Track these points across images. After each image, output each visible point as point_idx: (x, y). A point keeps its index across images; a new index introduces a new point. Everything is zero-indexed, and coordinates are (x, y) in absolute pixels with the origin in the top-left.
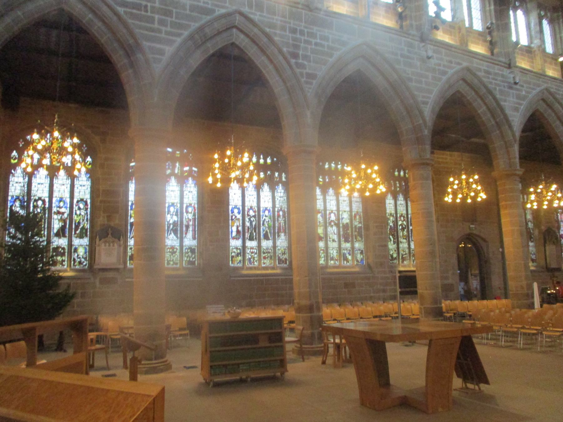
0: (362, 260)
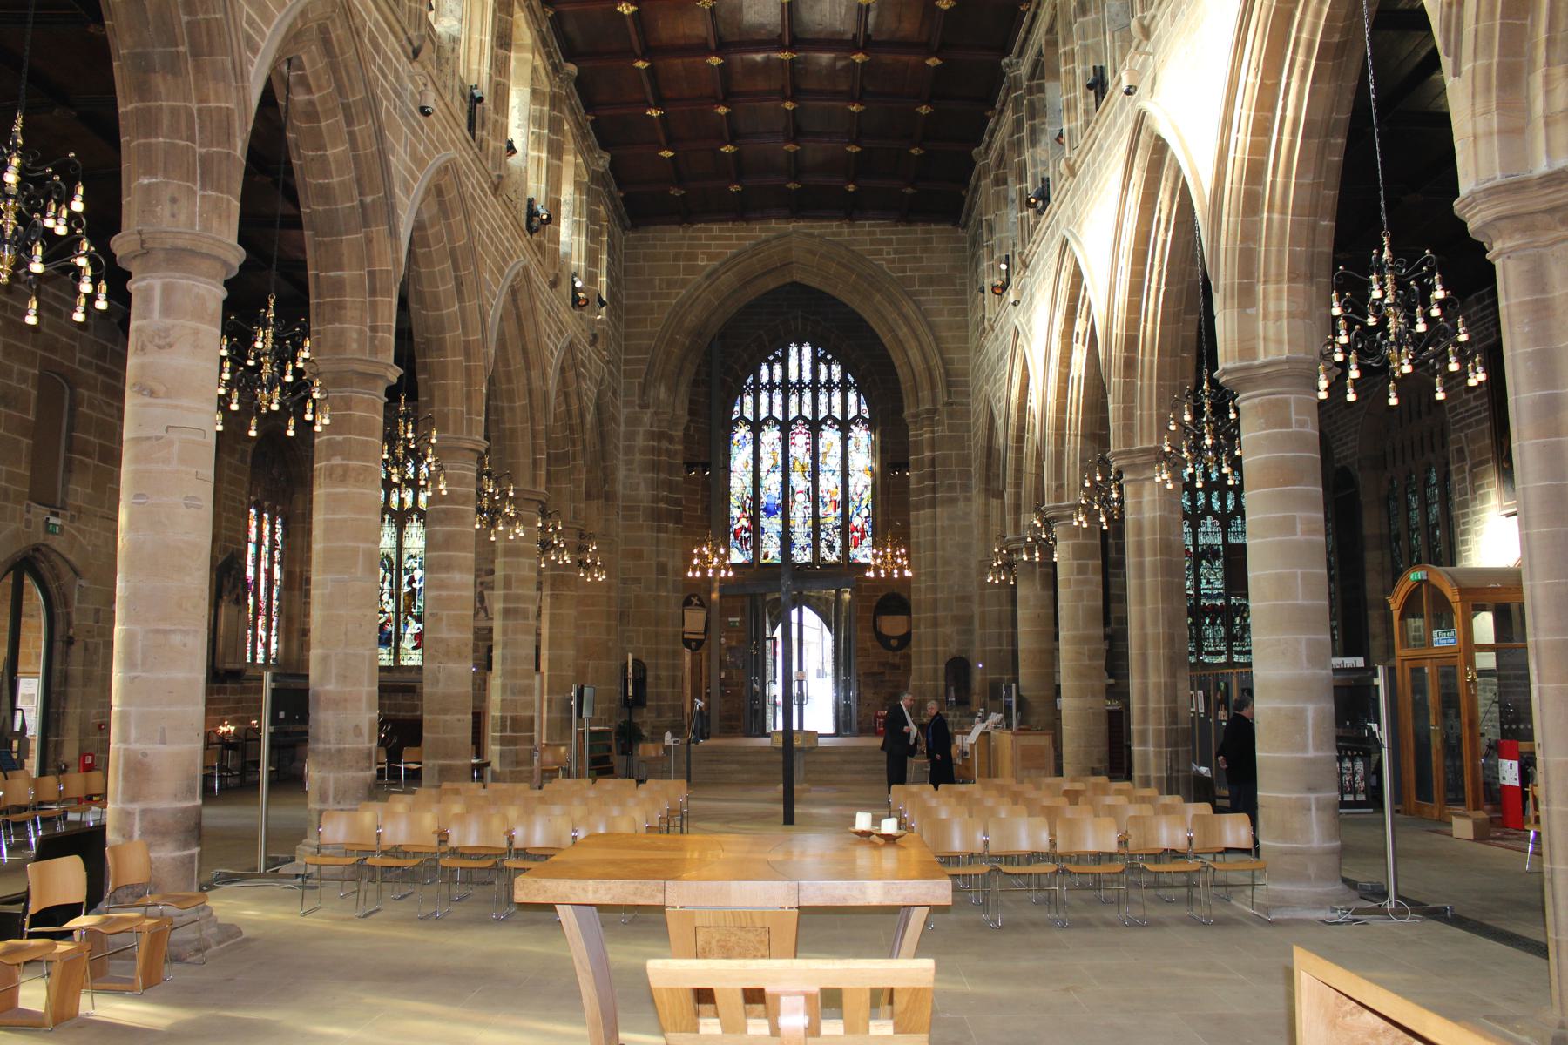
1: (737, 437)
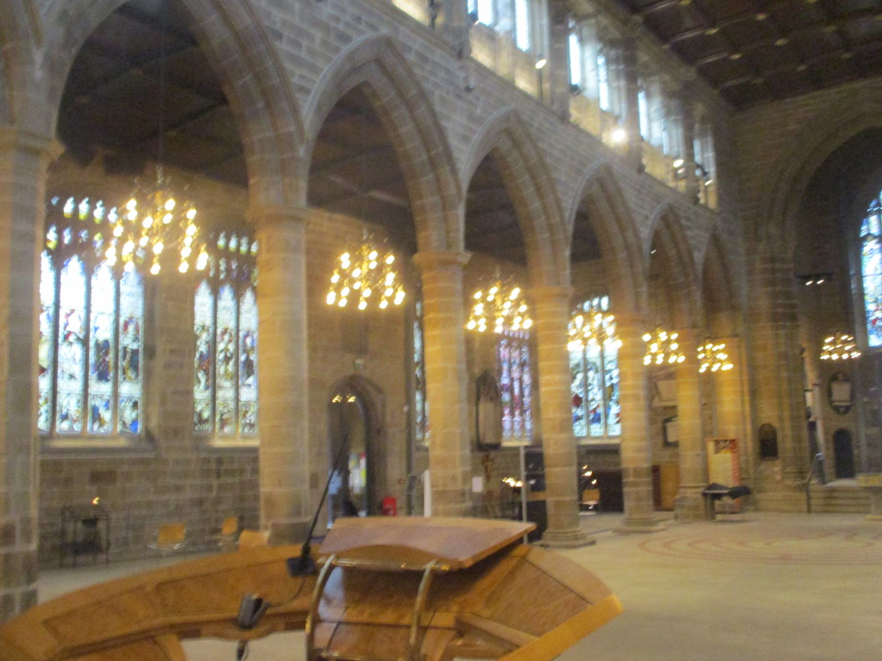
0: (135, 422)
1: (866, 250)
